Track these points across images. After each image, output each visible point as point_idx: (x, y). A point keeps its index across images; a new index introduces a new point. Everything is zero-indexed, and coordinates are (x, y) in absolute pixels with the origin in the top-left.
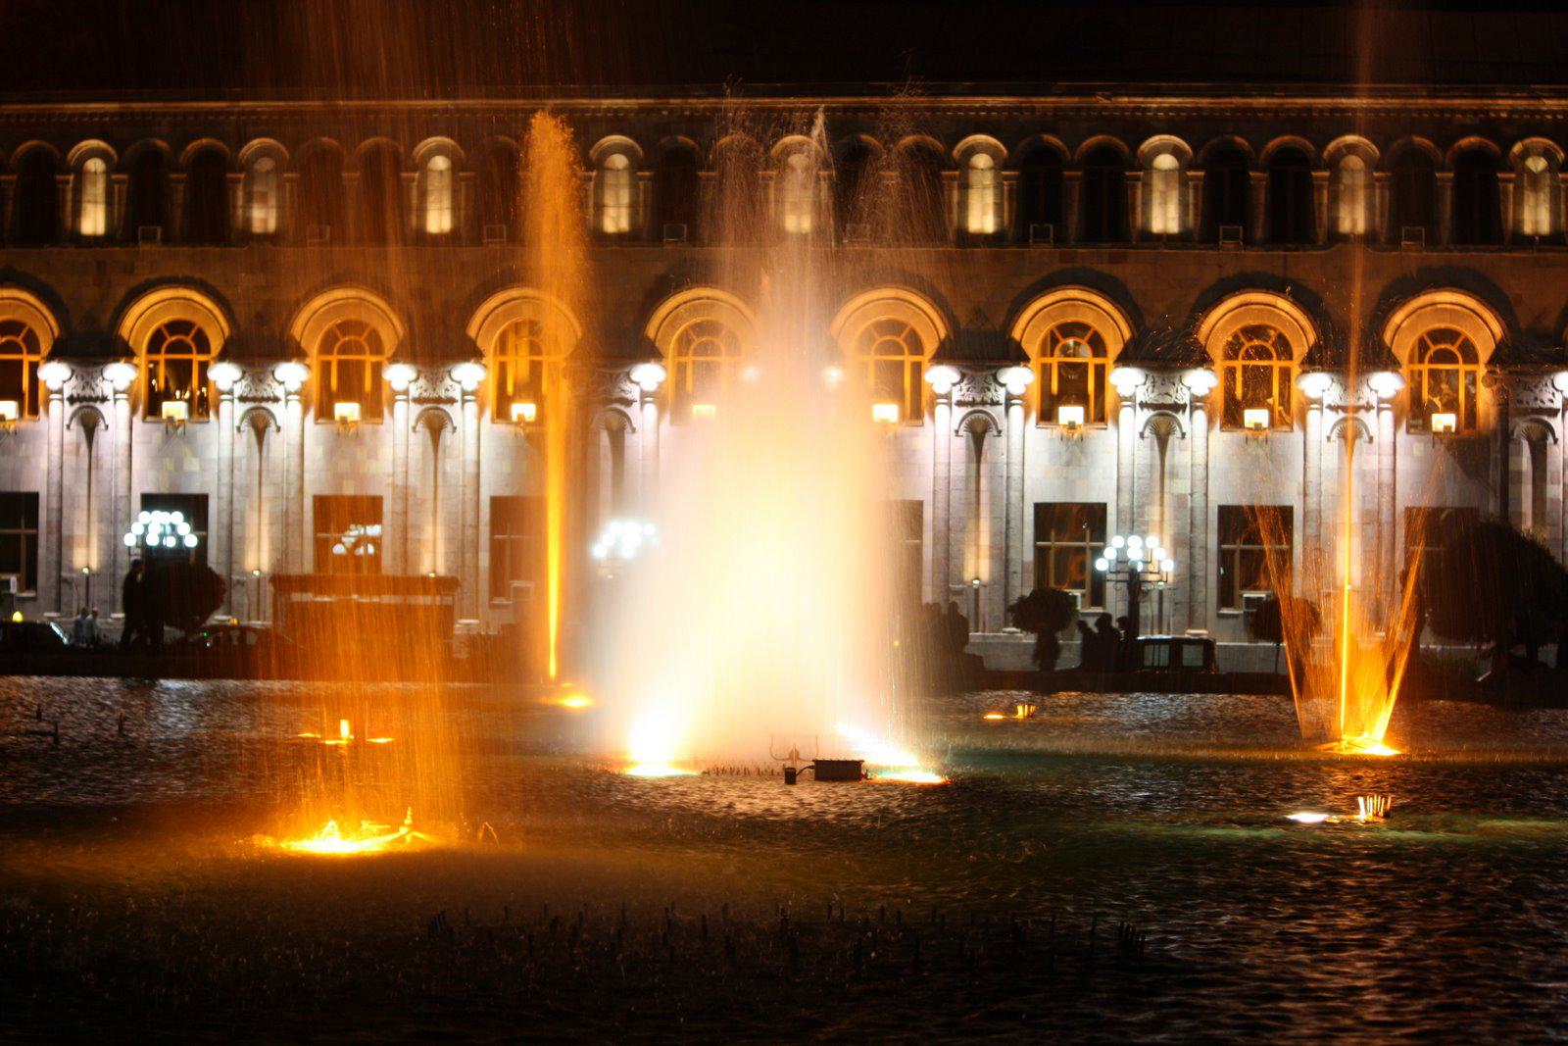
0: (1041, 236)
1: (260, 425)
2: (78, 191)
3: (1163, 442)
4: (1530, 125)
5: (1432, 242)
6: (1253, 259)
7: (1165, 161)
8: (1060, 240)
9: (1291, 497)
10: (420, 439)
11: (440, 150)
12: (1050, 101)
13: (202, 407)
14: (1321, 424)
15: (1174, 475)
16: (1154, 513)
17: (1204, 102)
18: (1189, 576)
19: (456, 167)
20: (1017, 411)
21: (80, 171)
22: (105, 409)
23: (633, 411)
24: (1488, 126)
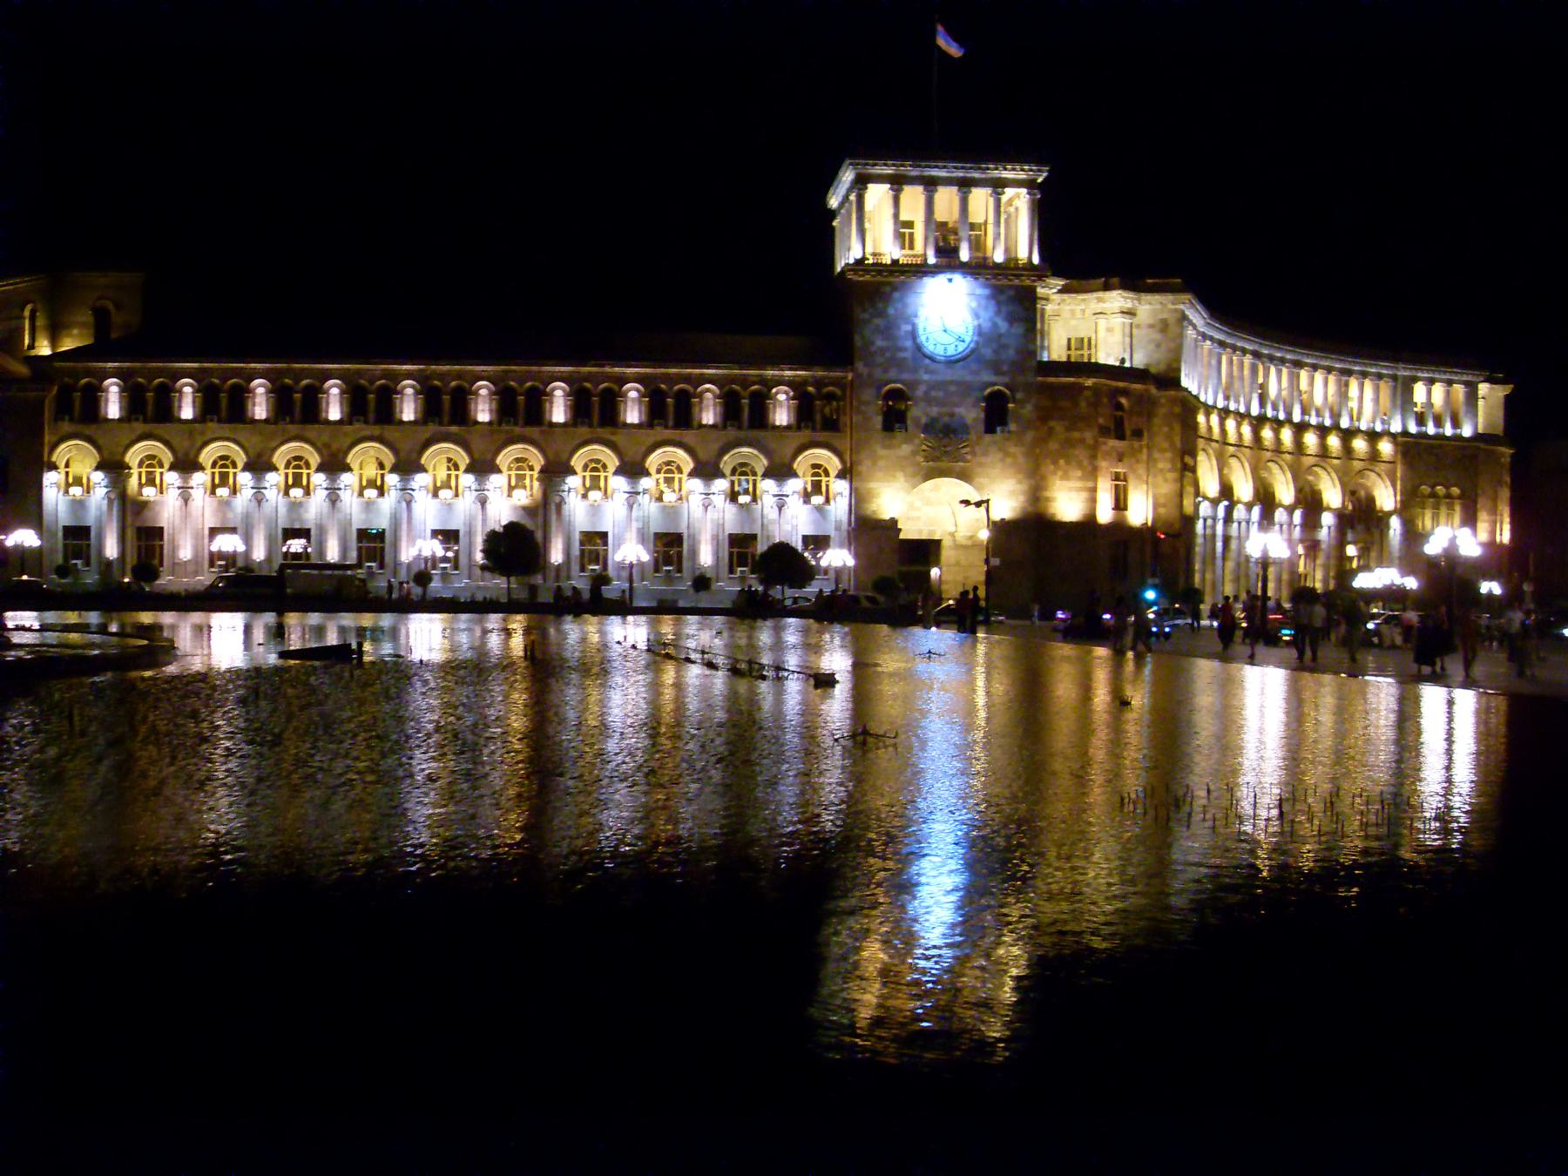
0: (583, 424)
1: (259, 499)
2: (180, 400)
3: (631, 507)
5: (740, 428)
7: (633, 394)
8: (591, 425)
9: (683, 529)
10: (326, 505)
13: (234, 491)
14: (695, 503)
16: (628, 536)
17: (648, 370)
19: (342, 392)
20: (572, 494)
21: (180, 392)
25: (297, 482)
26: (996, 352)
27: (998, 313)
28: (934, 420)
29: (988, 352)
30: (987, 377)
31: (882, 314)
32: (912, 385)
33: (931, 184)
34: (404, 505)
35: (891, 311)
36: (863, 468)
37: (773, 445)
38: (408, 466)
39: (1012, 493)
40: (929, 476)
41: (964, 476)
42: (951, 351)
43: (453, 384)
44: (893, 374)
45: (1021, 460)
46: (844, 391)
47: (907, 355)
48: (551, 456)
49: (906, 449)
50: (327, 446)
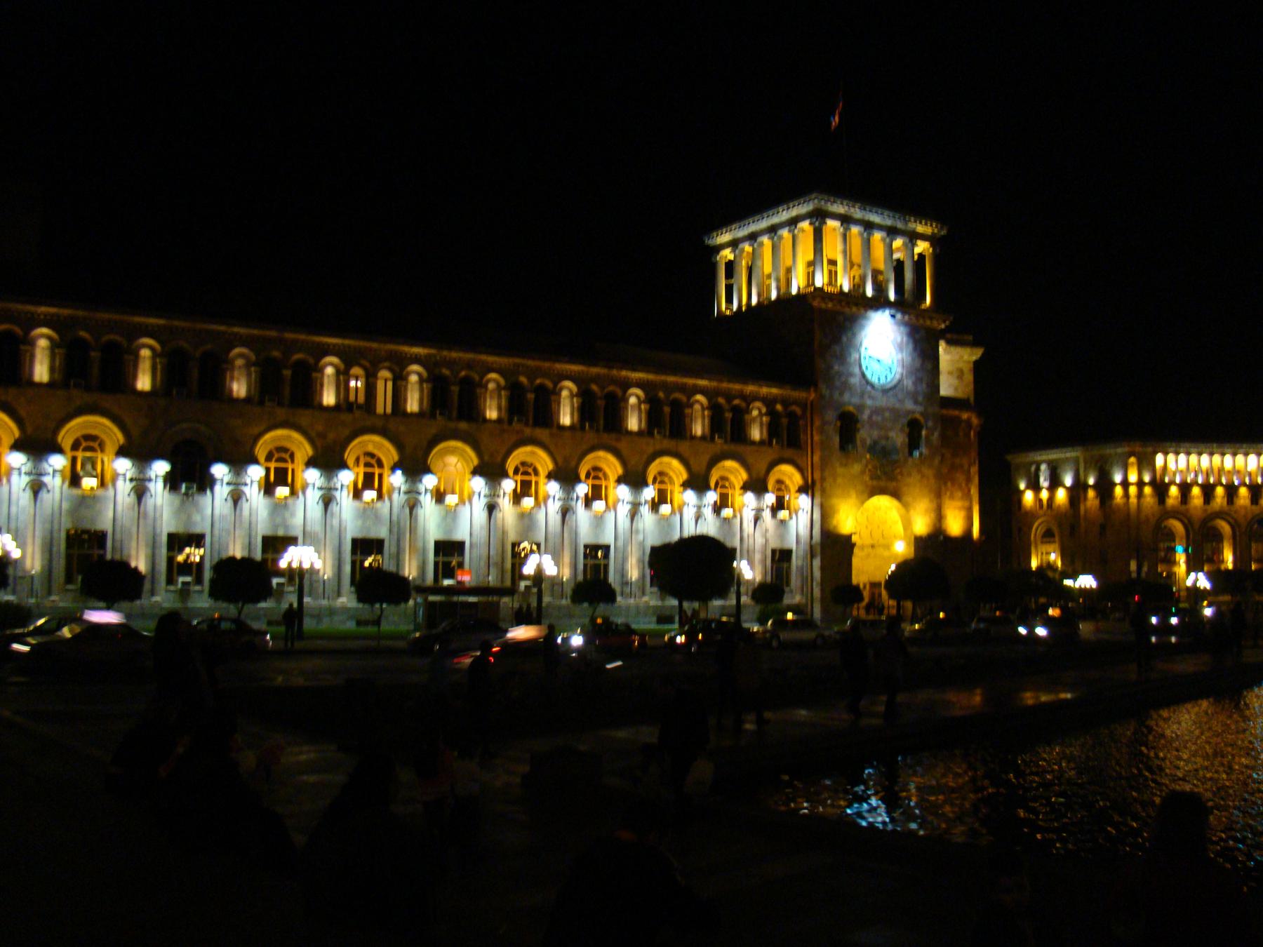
1: (236, 498)
4: (756, 398)
6: (667, 444)
11: (331, 364)
12: (595, 370)
15: (637, 532)
17: (651, 377)
18: (643, 577)
22: (151, 486)
23: (422, 498)
24: (743, 396)
25: (368, 482)
26: (915, 383)
27: (915, 349)
28: (875, 443)
29: (908, 383)
30: (909, 405)
31: (837, 339)
32: (860, 408)
33: (869, 226)
34: (407, 511)
35: (844, 339)
36: (827, 485)
37: (750, 460)
38: (415, 467)
39: (926, 511)
40: (873, 492)
41: (896, 494)
42: (883, 381)
43: (463, 373)
44: (846, 397)
45: (932, 481)
46: (804, 411)
47: (855, 381)
48: (560, 460)
49: (856, 468)
50: (322, 436)
